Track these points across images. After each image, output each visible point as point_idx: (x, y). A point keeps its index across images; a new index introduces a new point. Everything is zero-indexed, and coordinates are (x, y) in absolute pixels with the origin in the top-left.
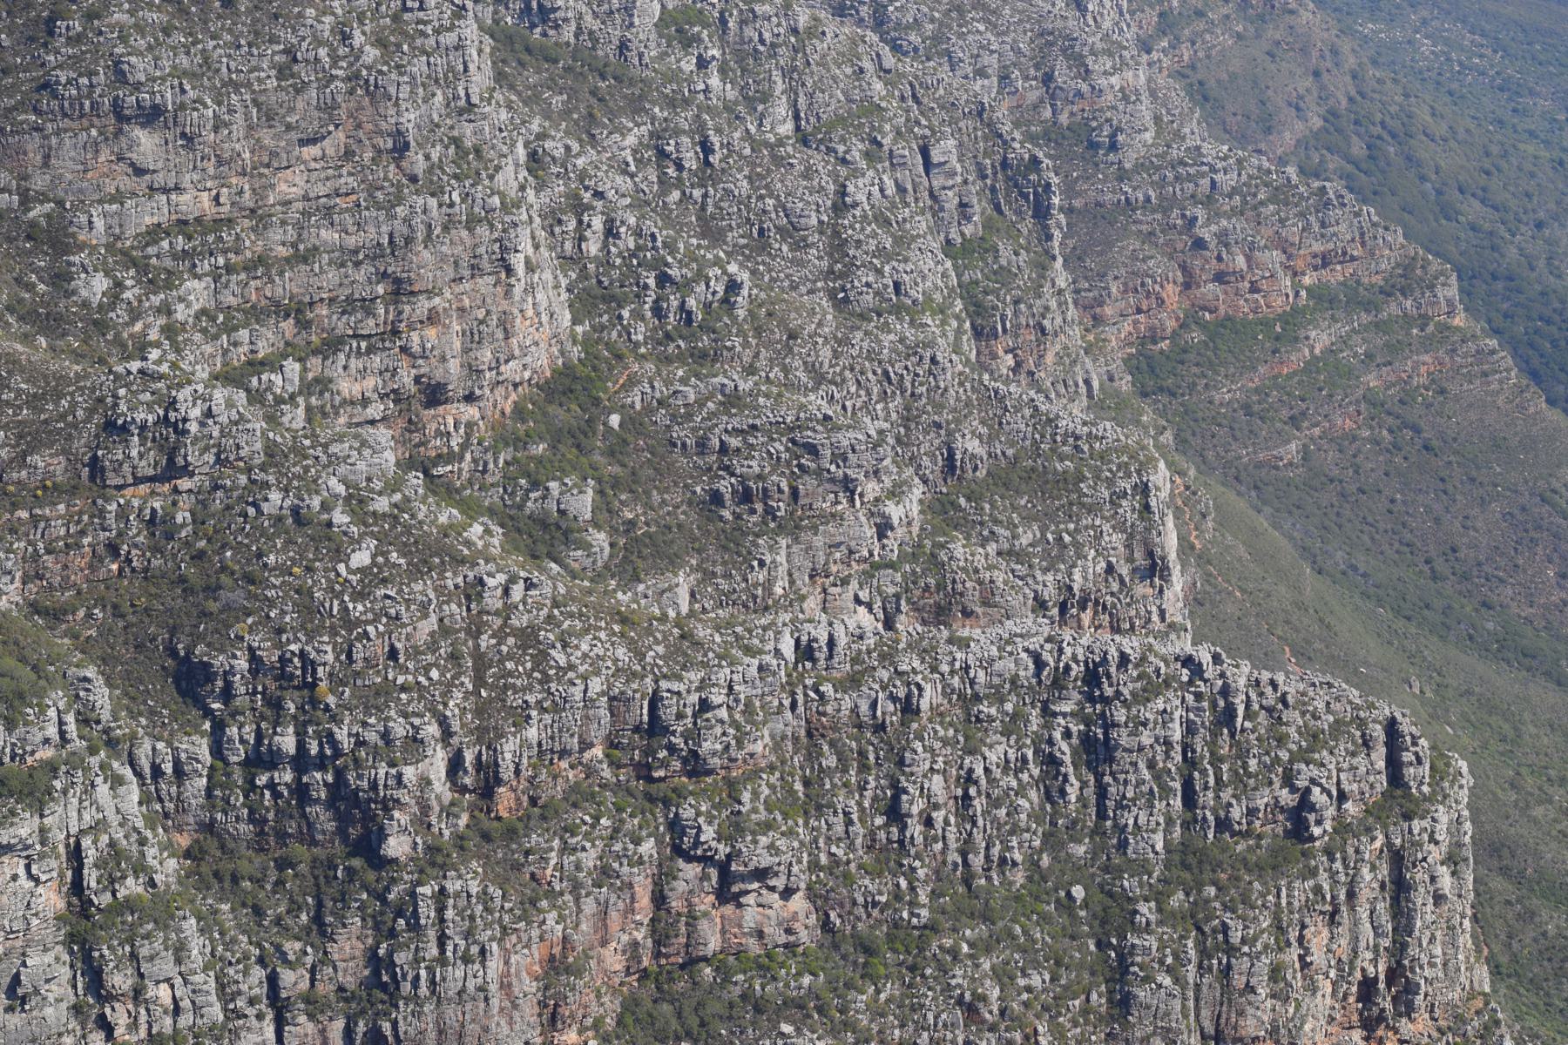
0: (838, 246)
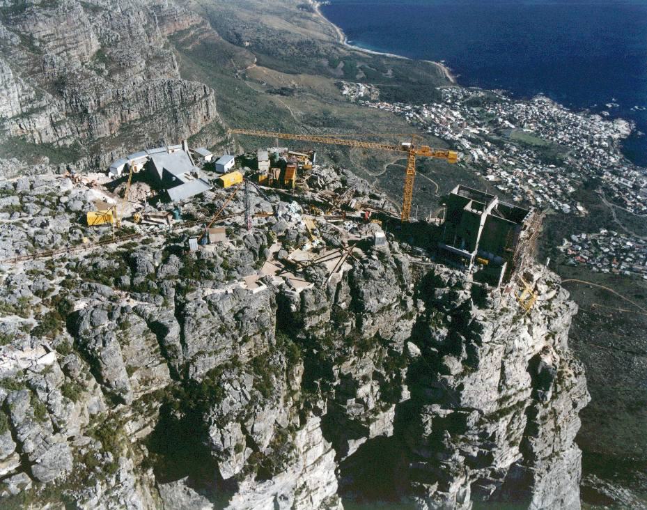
0: (129, 28)
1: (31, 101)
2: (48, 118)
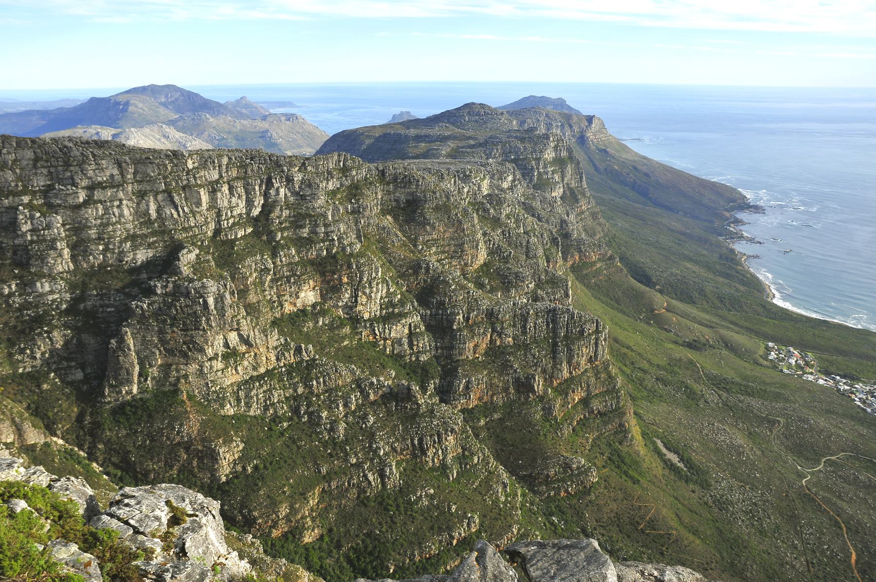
0: (527, 248)
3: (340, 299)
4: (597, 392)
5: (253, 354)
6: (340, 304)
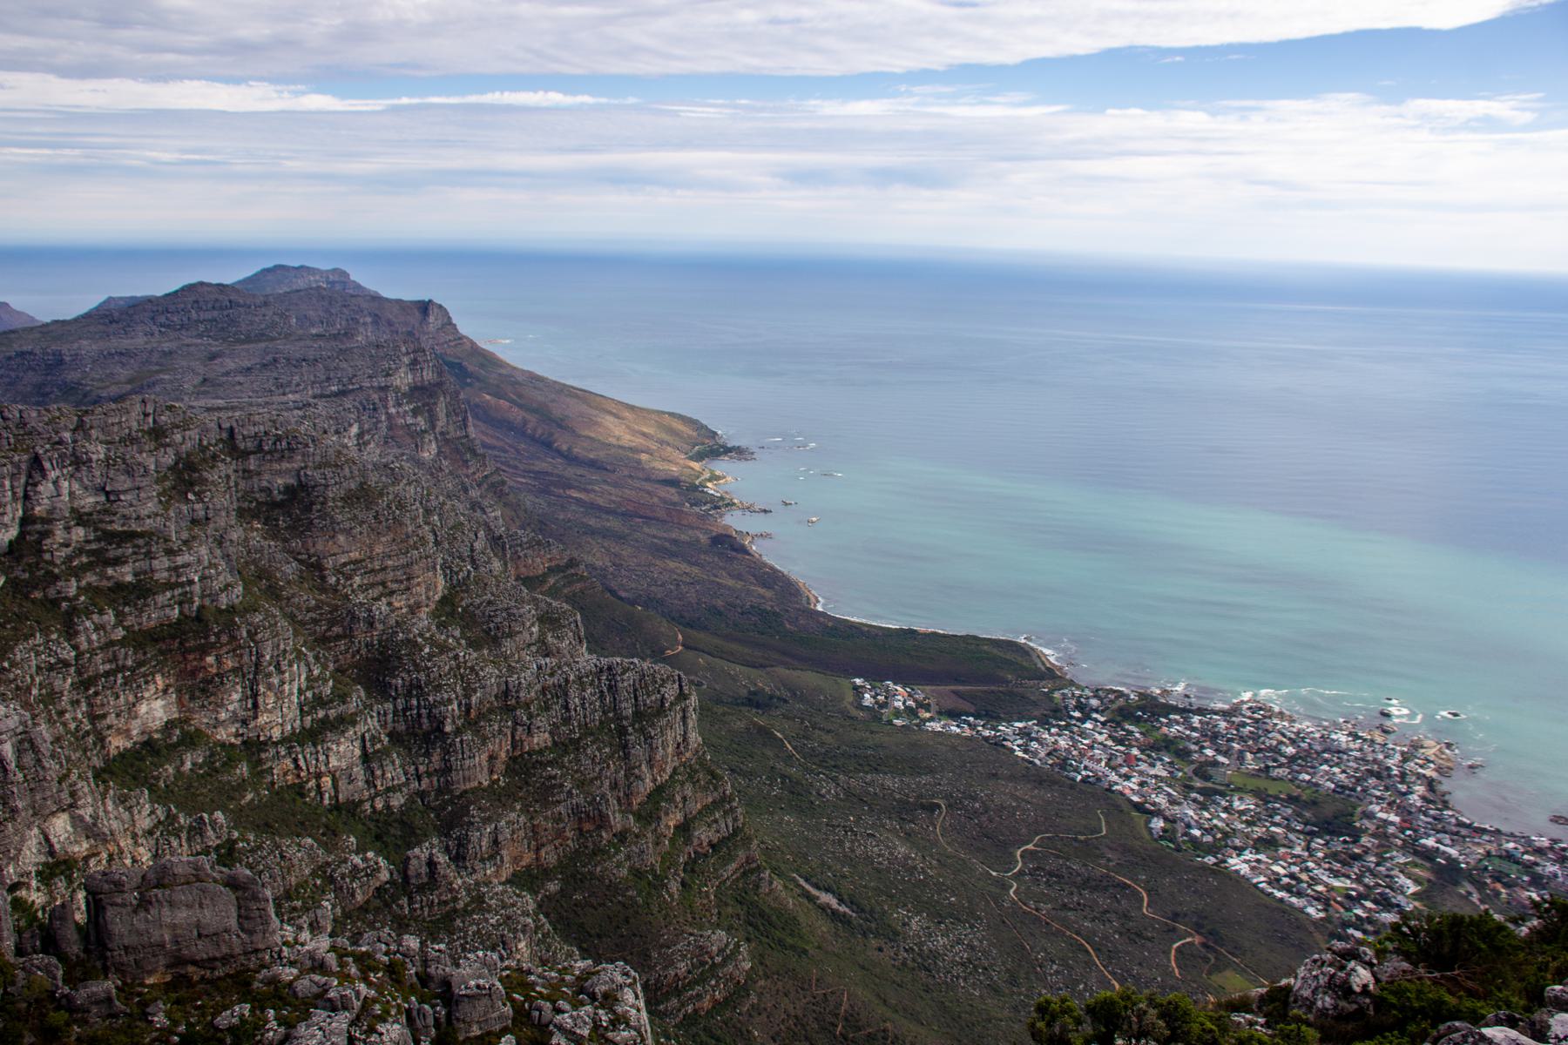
0: (473, 561)
1: (320, 702)
2: (357, 744)
3: (222, 705)
4: (699, 806)
5: (105, 855)
6: (223, 716)
